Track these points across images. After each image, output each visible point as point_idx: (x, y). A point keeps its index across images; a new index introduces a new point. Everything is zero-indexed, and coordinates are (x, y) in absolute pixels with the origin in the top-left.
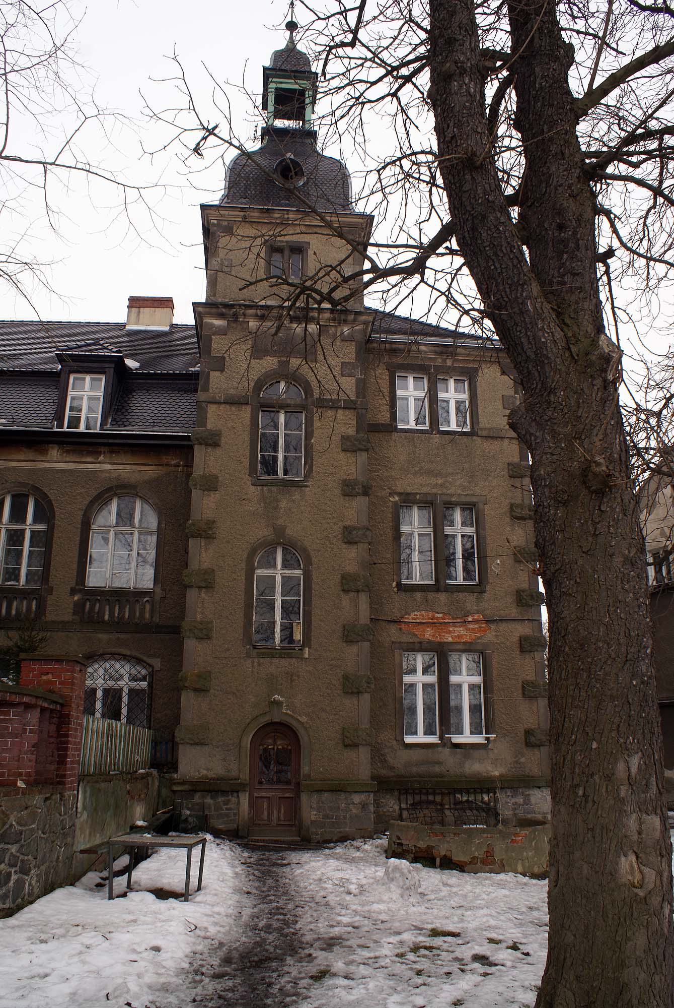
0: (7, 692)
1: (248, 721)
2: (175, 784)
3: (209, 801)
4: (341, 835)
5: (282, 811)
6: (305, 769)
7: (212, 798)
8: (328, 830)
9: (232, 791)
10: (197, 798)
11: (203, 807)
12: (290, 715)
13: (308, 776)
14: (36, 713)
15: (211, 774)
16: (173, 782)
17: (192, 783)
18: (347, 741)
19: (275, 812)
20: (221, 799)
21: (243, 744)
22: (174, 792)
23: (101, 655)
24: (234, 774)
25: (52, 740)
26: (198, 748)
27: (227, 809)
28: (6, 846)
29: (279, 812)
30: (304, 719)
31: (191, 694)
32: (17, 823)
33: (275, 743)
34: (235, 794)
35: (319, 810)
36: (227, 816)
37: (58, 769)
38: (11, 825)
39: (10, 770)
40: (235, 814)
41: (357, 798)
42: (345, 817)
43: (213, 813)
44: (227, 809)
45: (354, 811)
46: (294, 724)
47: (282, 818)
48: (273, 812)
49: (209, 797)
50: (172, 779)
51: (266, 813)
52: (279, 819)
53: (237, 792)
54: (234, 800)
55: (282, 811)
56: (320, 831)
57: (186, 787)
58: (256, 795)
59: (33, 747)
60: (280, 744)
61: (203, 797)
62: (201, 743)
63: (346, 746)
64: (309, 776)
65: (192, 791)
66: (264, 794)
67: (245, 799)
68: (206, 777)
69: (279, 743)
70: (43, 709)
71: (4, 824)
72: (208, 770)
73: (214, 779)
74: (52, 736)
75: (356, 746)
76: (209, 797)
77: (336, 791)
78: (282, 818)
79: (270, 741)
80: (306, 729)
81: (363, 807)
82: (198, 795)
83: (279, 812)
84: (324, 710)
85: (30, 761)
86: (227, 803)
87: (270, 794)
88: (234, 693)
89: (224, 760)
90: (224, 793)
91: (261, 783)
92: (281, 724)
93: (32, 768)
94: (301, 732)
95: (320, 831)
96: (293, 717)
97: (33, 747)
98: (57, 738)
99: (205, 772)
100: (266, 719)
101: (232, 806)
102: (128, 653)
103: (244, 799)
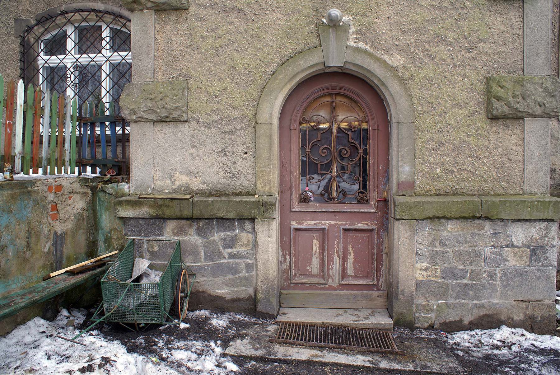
1: (273, 68)
2: (120, 203)
3: (192, 238)
4: (482, 312)
5: (351, 259)
6: (402, 170)
7: (200, 232)
8: (452, 301)
9: (242, 219)
10: (169, 233)
11: (179, 250)
12: (365, 52)
13: (408, 187)
15: (197, 184)
16: (120, 201)
17: (155, 202)
18: (500, 108)
19: (336, 259)
20: (218, 236)
21: (262, 117)
22: (122, 218)
23: (64, 13)
24: (244, 182)
26: (169, 129)
27: (231, 256)
29: (344, 259)
30: (396, 60)
31: (150, 17)
33: (333, 117)
34: (248, 226)
35: (433, 258)
36: (234, 269)
40: (249, 267)
41: (519, 234)
42: (491, 276)
43: (203, 263)
44: (231, 256)
45: (513, 262)
46: (375, 67)
47: (350, 271)
48: (330, 260)
49: (193, 231)
50: (119, 195)
51: (316, 261)
52: (344, 274)
53: (252, 220)
54: (245, 236)
55: (351, 259)
56: (434, 303)
57: (144, 211)
58: (294, 224)
60: (345, 118)
61: (181, 231)
62: (177, 121)
63: (494, 118)
64: (412, 185)
65: (157, 217)
66: (312, 223)
67: (268, 236)
68: (188, 189)
69: (340, 118)
72: (190, 173)
73: (201, 193)
75: (517, 117)
76: (193, 231)
77: (474, 218)
78: (350, 271)
79: (323, 113)
80: (402, 81)
81: (533, 252)
82: (171, 226)
83: (344, 259)
84: (441, 39)
86: (231, 242)
87: (325, 224)
88: (239, 10)
89: (224, 152)
90: (223, 222)
91: (304, 200)
92: (343, 74)
94: (393, 91)
95: (434, 303)
96: (371, 55)
99: (183, 180)
100: (310, 63)
101: (243, 250)
102: (101, 6)
103: (268, 236)
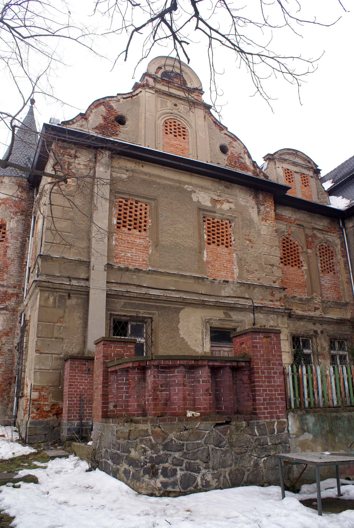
0: (161, 360)
14: (228, 370)
25: (246, 385)
28: (168, 453)
32: (177, 438)
37: (253, 405)
38: (172, 440)
39: (179, 406)
59: (206, 391)
70: (184, 366)
71: (164, 439)
74: (246, 383)
85: (205, 400)
93: (207, 404)
97: (206, 391)
98: (250, 384)
